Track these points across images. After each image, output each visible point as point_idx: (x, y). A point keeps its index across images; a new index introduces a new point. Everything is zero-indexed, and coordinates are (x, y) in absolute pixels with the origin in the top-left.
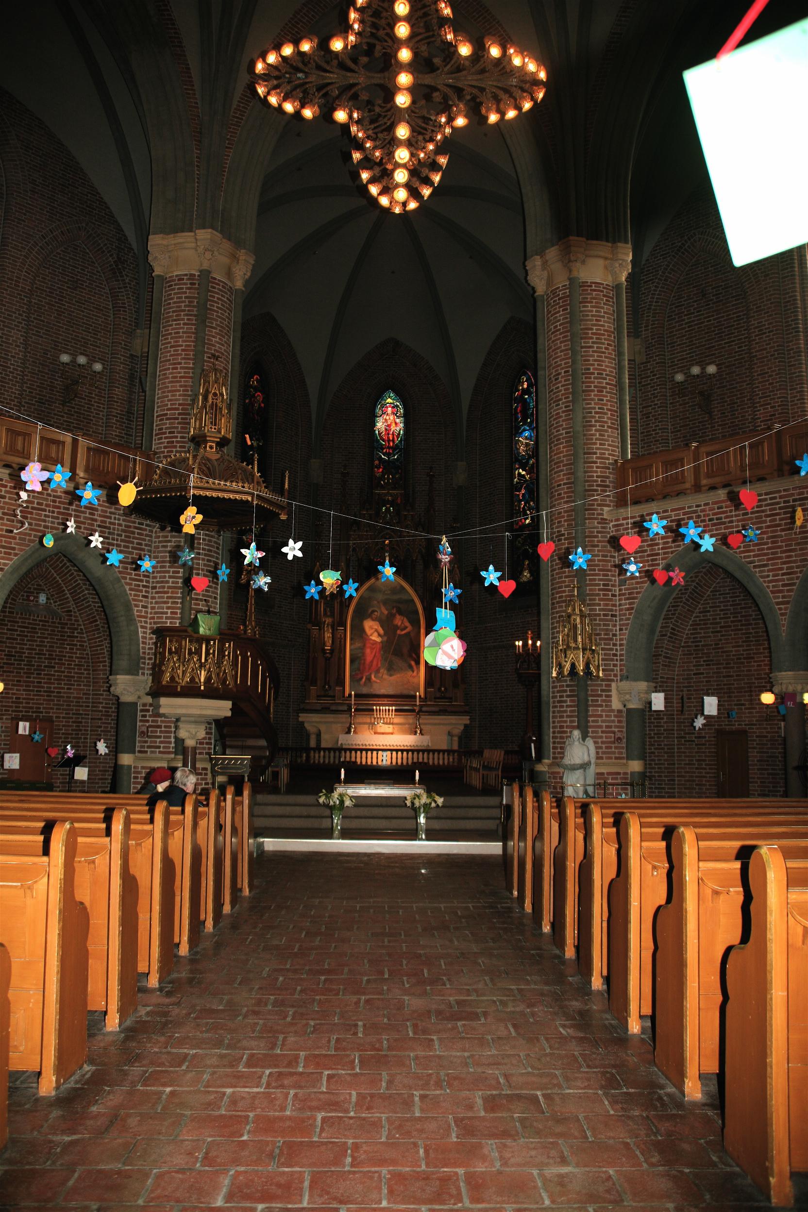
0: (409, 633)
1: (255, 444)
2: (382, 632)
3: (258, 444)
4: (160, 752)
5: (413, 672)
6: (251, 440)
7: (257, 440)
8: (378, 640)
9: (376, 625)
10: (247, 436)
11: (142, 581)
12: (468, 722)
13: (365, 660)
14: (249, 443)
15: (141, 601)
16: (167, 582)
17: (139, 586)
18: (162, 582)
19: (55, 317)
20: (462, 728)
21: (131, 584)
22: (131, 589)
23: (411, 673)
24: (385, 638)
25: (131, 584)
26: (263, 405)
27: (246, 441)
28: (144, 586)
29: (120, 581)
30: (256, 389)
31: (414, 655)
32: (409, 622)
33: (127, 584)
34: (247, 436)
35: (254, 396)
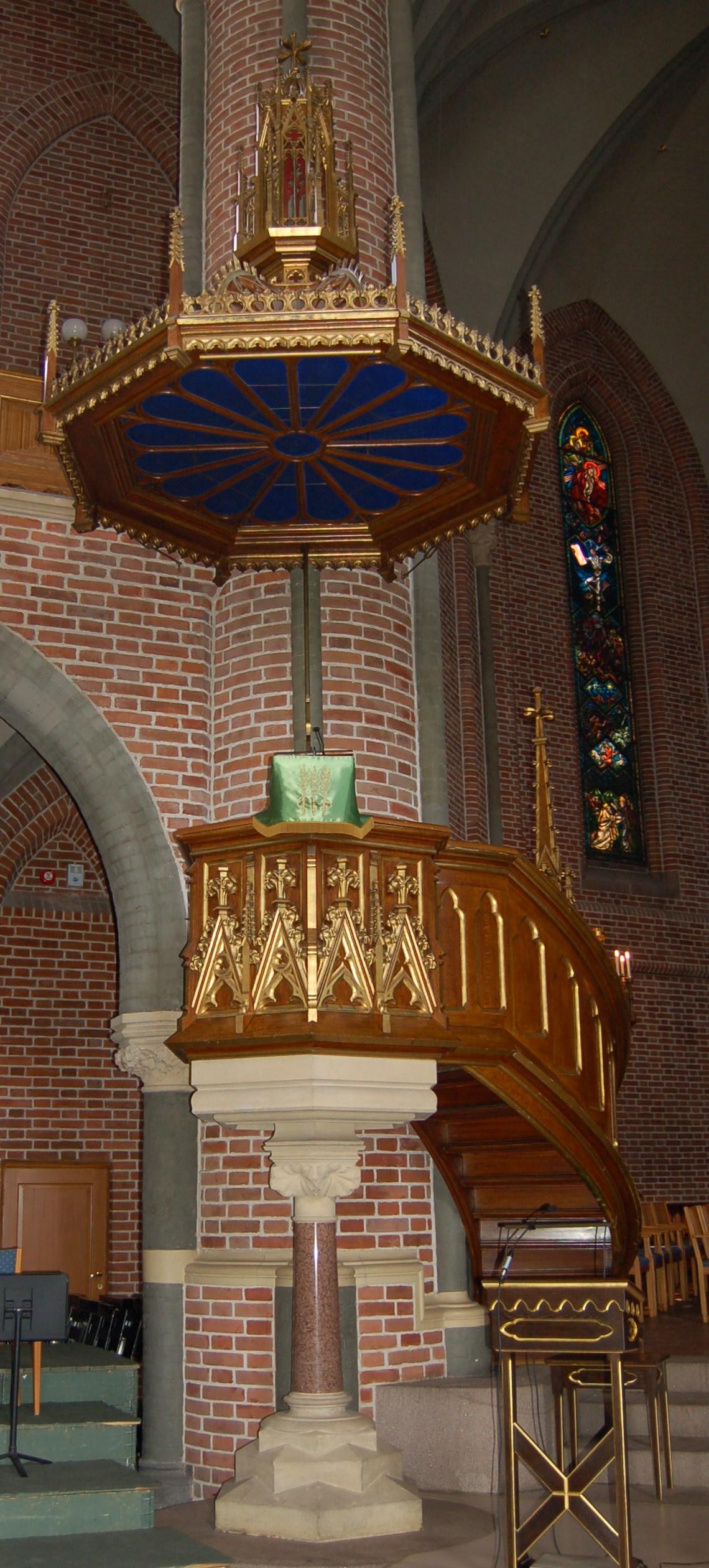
1: (596, 562)
3: (603, 565)
4: (258, 1242)
6: (586, 554)
7: (600, 553)
10: (576, 548)
11: (182, 738)
14: (582, 560)
15: (183, 794)
16: (254, 732)
17: (173, 751)
18: (240, 735)
19: (64, 269)
21: (148, 748)
22: (146, 763)
25: (148, 748)
26: (602, 485)
27: (574, 559)
28: (187, 752)
29: (113, 741)
30: (581, 453)
33: (134, 747)
34: (576, 548)
35: (580, 469)
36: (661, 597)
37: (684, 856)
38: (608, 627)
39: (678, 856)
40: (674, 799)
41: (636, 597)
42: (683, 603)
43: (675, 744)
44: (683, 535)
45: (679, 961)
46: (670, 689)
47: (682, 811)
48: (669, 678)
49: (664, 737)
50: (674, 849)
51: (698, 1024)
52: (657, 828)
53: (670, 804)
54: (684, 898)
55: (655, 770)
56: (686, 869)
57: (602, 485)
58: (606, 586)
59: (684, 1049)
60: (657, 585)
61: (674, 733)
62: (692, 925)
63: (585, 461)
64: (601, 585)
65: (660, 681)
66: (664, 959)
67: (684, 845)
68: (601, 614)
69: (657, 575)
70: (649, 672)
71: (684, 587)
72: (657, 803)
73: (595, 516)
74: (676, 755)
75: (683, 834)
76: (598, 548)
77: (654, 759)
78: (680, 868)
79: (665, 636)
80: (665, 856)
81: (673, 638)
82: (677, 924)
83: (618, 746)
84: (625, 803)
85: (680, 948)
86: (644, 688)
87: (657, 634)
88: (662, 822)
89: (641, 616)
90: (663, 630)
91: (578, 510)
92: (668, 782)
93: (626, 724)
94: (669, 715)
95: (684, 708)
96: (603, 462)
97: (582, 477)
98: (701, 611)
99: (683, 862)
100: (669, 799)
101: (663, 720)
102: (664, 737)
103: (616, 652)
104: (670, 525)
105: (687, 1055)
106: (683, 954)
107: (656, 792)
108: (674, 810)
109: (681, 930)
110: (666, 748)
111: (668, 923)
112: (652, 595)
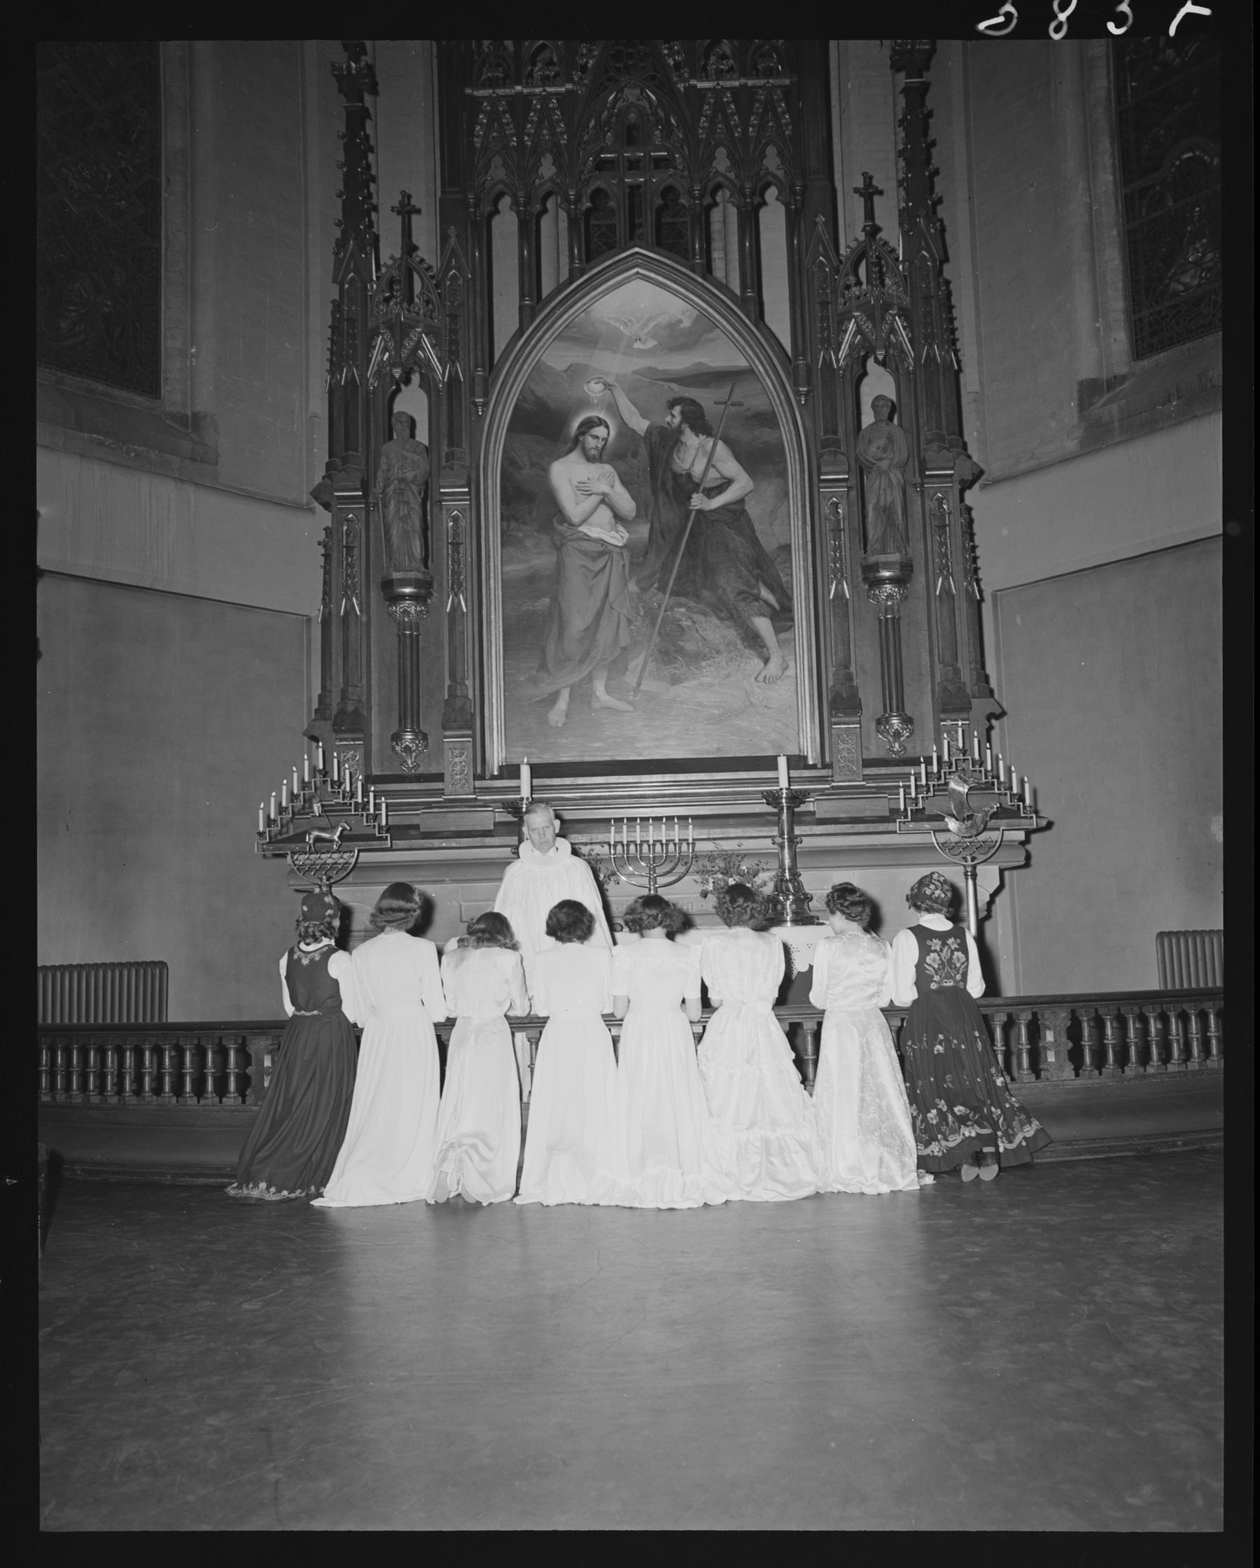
0: (741, 501)
2: (626, 503)
5: (766, 661)
8: (617, 537)
9: (603, 478)
23: (757, 663)
24: (644, 530)
31: (765, 593)
32: (738, 457)
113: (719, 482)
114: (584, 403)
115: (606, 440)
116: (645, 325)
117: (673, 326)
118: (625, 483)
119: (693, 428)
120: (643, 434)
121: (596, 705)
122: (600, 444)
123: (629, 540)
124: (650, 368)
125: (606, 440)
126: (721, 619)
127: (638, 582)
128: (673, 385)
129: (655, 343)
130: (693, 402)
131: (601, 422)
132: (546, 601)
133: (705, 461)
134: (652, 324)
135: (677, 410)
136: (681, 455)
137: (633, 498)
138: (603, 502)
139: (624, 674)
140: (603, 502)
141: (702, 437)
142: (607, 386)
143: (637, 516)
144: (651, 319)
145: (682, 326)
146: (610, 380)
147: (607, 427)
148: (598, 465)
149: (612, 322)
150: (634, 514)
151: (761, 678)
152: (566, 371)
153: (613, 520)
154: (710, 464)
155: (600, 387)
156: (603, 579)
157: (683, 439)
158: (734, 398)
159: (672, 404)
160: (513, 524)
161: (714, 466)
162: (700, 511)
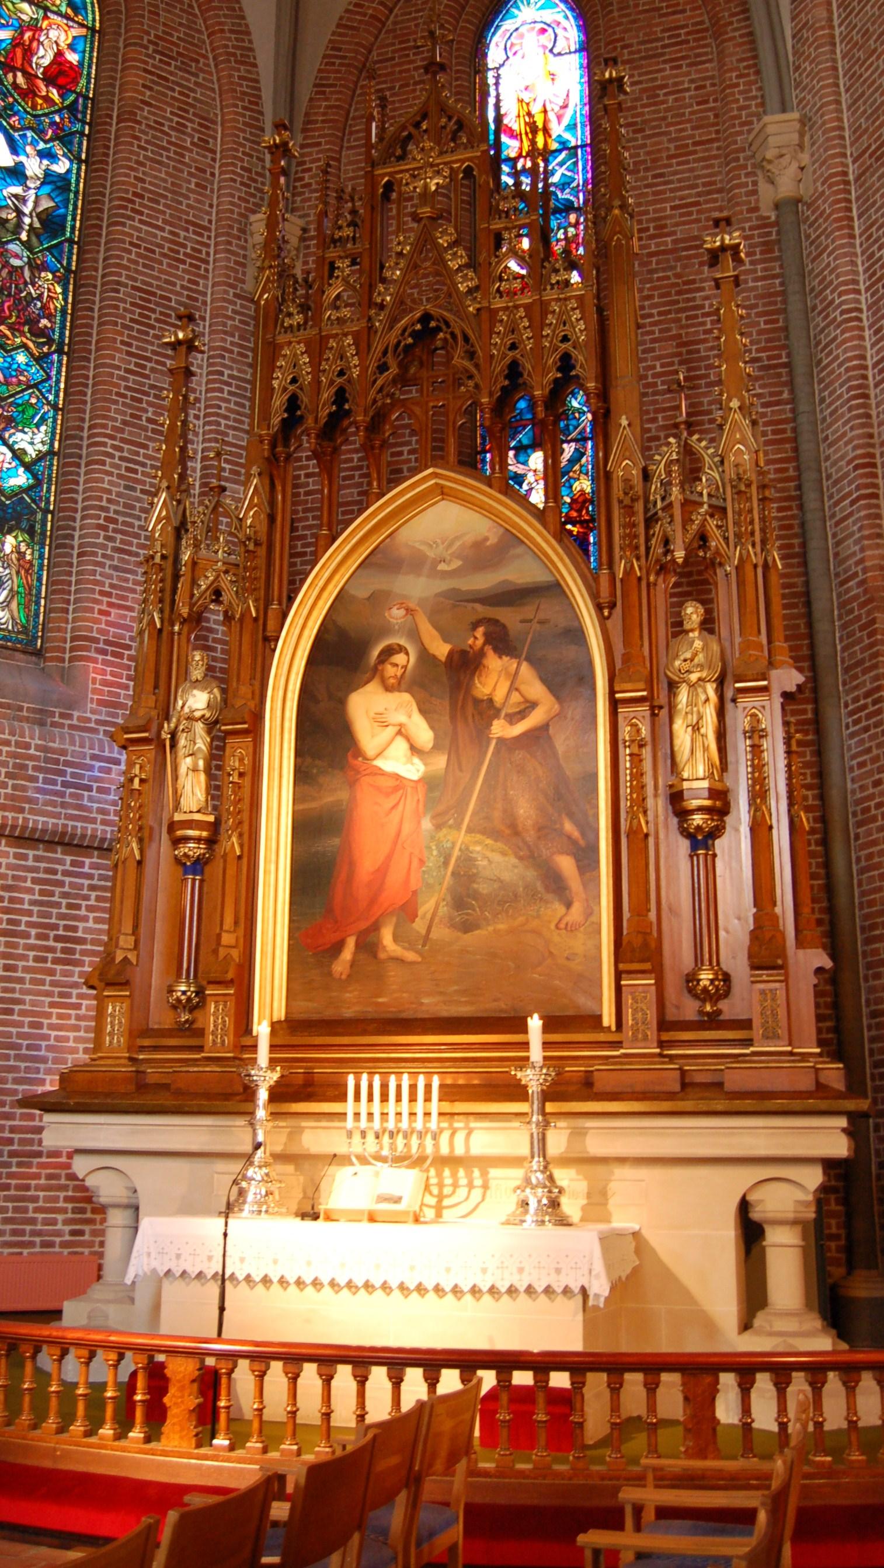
1: (34, 167)
2: (423, 733)
3: (47, 173)
5: (569, 905)
8: (413, 770)
12: (839, 1147)
13: (352, 864)
20: (813, 1178)
23: (561, 909)
31: (568, 827)
32: (544, 681)
35: (35, 28)
36: (139, 230)
37: (107, 642)
38: (37, 268)
39: (96, 640)
40: (104, 547)
41: (100, 227)
42: (185, 246)
43: (121, 458)
44: (203, 145)
45: (57, 816)
46: (127, 371)
47: (115, 568)
48: (129, 353)
49: (105, 444)
50: (91, 630)
51: (86, 930)
52: (69, 593)
53: (95, 554)
54: (93, 712)
55: (80, 498)
56: (105, 662)
57: (73, 58)
58: (46, 204)
59: (51, 972)
60: (133, 210)
61: (122, 440)
62: (94, 757)
63: (46, 17)
64: (36, 203)
65: (113, 358)
66: (21, 810)
67: (108, 623)
68: (27, 245)
69: (135, 194)
70: (97, 342)
71: (187, 222)
72: (75, 552)
73: (47, 99)
74: (120, 476)
75: (110, 605)
76: (42, 146)
77: (82, 480)
78: (95, 661)
79: (134, 288)
80: (73, 639)
81: (154, 294)
82: (64, 753)
83: (18, 455)
84: (18, 547)
85: (62, 795)
86: (87, 368)
87: (118, 283)
88: (77, 582)
89: (101, 256)
90: (135, 280)
91: (15, 85)
92: (99, 517)
93: (43, 420)
94: (117, 411)
95: (149, 403)
96: (82, 25)
97: (32, 40)
98: (215, 261)
99: (104, 652)
100: (95, 545)
101: (105, 417)
102: (105, 444)
103: (44, 307)
104: (180, 128)
105: (53, 984)
106: (63, 805)
107: (77, 534)
108: (102, 565)
109: (67, 763)
110: (103, 463)
111: (38, 748)
112: (123, 224)
113: (523, 707)
114: (386, 630)
115: (405, 667)
116: (450, 545)
117: (478, 545)
118: (422, 711)
119: (496, 650)
120: (443, 659)
121: (382, 955)
122: (399, 674)
123: (425, 773)
124: (454, 589)
125: (405, 667)
126: (521, 858)
127: (433, 818)
128: (478, 607)
129: (460, 563)
130: (497, 621)
131: (401, 649)
132: (336, 841)
133: (508, 684)
134: (458, 544)
135: (480, 632)
136: (483, 679)
137: (432, 728)
138: (399, 733)
139: (413, 921)
140: (399, 733)
141: (505, 659)
142: (409, 611)
143: (434, 747)
144: (457, 538)
145: (488, 543)
146: (412, 605)
147: (407, 654)
148: (397, 694)
149: (417, 545)
150: (431, 745)
151: (562, 926)
152: (369, 598)
153: (409, 753)
154: (513, 688)
155: (402, 612)
156: (395, 816)
157: (485, 662)
158: (541, 615)
159: (475, 626)
160: (309, 760)
161: (517, 689)
162: (501, 741)
